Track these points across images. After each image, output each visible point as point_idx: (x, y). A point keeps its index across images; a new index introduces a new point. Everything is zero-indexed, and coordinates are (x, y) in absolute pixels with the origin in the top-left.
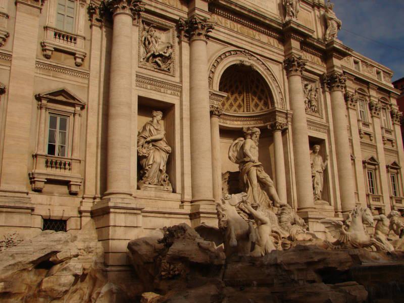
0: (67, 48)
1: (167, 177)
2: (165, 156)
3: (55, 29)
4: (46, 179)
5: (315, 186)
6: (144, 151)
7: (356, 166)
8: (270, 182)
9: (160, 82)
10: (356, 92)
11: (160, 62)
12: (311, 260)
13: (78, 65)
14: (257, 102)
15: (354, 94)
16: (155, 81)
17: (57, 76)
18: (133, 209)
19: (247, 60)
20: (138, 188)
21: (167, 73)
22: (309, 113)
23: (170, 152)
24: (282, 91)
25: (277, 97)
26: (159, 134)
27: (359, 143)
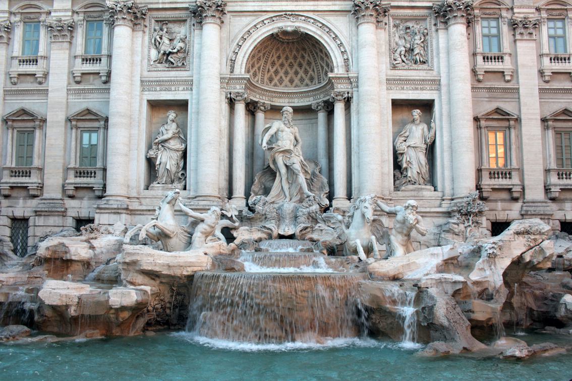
2: (177, 156)
5: (405, 165)
6: (152, 153)
7: (523, 129)
9: (168, 81)
10: (538, 10)
11: (172, 60)
13: (106, 82)
14: (327, 69)
15: (531, 16)
17: (87, 97)
18: (115, 209)
19: (289, 24)
21: (179, 69)
22: (406, 67)
24: (348, 49)
25: (337, 58)
26: (167, 133)
27: (537, 91)
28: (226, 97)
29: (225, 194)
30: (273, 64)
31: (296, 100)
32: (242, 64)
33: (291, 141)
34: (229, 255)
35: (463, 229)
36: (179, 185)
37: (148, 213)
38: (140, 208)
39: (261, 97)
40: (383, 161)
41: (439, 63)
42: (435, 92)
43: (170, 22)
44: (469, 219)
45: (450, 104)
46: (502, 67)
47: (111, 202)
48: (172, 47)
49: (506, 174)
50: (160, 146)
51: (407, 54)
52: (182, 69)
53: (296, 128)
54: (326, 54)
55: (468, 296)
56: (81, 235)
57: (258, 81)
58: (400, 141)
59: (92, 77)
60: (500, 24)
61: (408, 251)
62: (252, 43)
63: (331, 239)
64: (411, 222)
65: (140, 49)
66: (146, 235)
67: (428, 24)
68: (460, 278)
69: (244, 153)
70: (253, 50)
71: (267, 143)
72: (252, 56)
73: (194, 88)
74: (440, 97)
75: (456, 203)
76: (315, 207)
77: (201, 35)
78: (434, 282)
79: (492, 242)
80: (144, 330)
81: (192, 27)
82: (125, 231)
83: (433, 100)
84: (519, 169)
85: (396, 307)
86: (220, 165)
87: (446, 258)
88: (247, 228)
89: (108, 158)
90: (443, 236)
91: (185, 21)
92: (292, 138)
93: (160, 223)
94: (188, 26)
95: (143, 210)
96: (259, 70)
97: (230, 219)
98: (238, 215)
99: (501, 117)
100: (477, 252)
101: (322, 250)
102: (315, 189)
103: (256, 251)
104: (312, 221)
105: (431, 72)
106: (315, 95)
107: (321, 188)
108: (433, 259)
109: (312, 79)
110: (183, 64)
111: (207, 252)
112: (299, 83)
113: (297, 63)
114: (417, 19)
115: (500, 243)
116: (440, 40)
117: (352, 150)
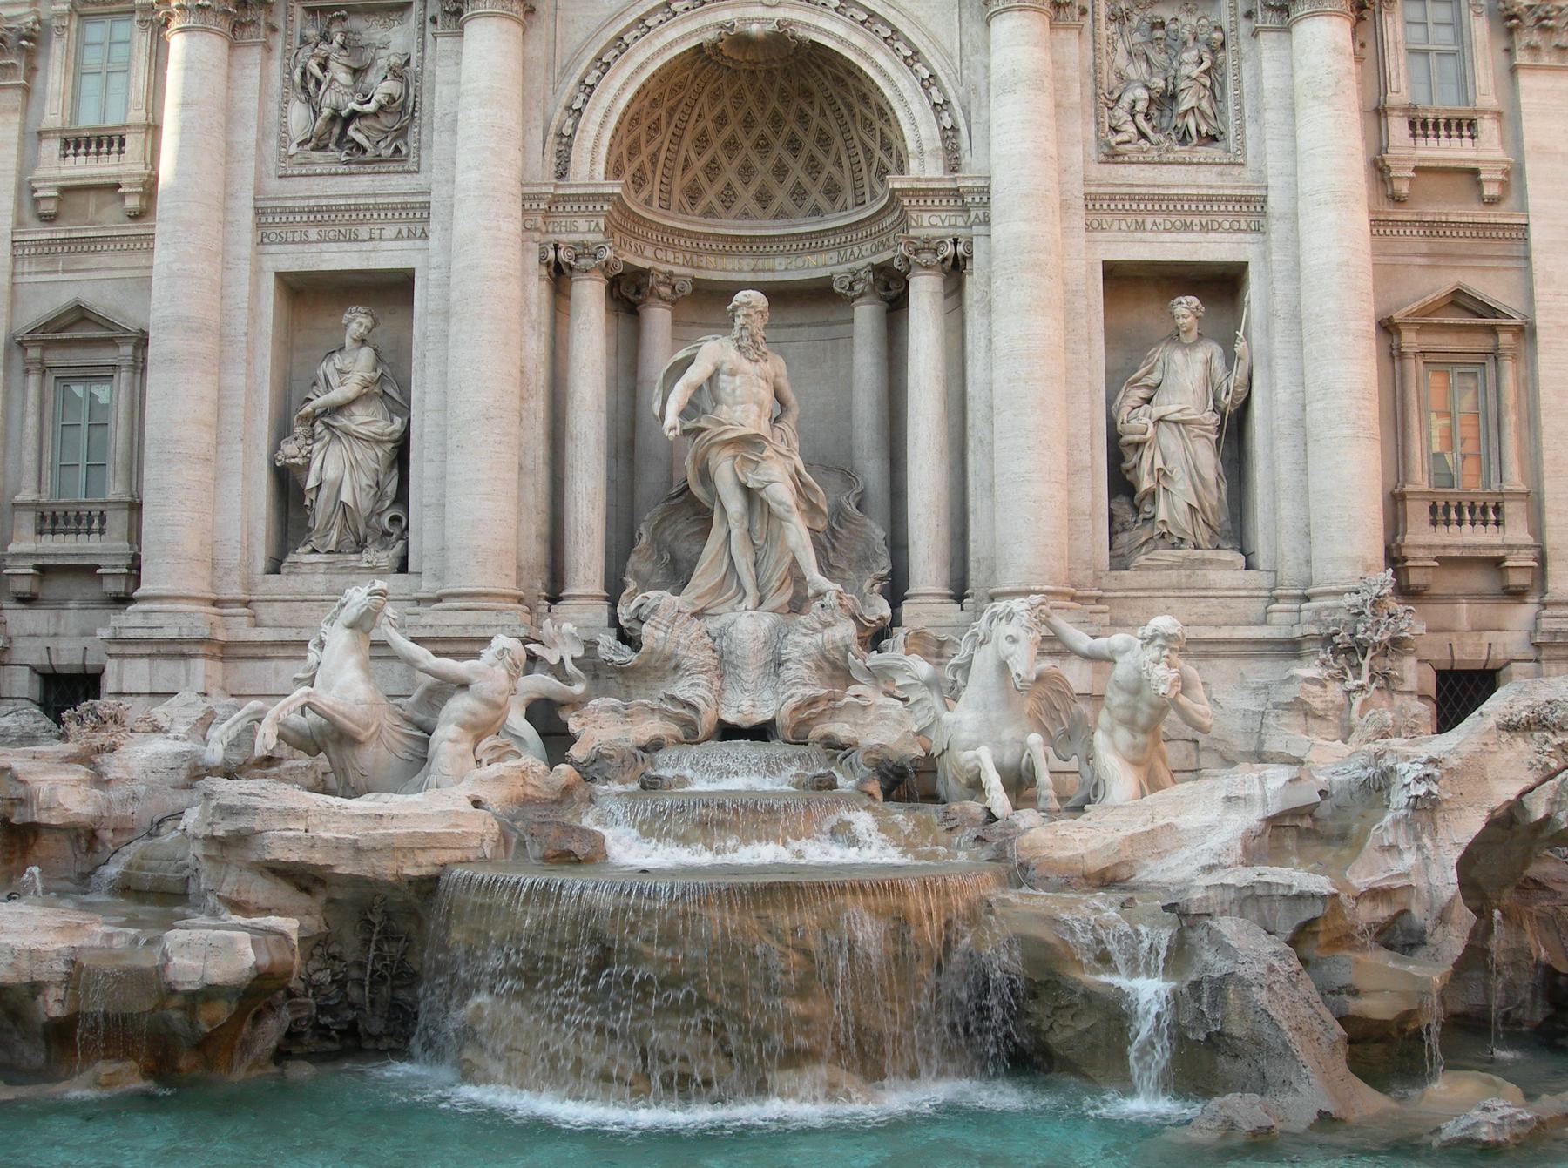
0: (94, 177)
1: (395, 520)
2: (373, 458)
3: (61, 131)
4: (36, 567)
5: (1146, 484)
8: (780, 503)
11: (360, 138)
12: (208, 832)
13: (137, 216)
14: (885, 160)
16: (329, 209)
20: (275, 568)
21: (384, 167)
23: (396, 436)
26: (342, 384)
28: (542, 259)
29: (539, 586)
30: (702, 141)
31: (779, 262)
32: (595, 146)
33: (760, 405)
34: (554, 802)
35: (1340, 699)
36: (383, 554)
37: (282, 652)
39: (660, 254)
40: (1073, 471)
42: (1248, 237)
44: (1359, 665)
45: (1299, 279)
46: (1472, 155)
47: (155, 620)
48: (359, 97)
49: (1484, 510)
50: (319, 427)
51: (1154, 112)
52: (394, 166)
53: (780, 361)
54: (880, 109)
55: (1345, 939)
56: (63, 737)
57: (648, 202)
58: (1131, 402)
59: (92, 200)
60: (1464, 12)
61: (1152, 783)
62: (631, 78)
63: (896, 737)
64: (1162, 689)
65: (255, 104)
66: (280, 736)
68: (1320, 884)
69: (603, 447)
70: (632, 100)
71: (684, 414)
72: (631, 119)
73: (434, 226)
74: (1265, 256)
75: (1317, 612)
76: (845, 631)
77: (459, 53)
78: (1232, 895)
79: (1425, 757)
80: (281, 1055)
81: (430, 28)
82: (207, 721)
83: (1244, 266)
84: (1527, 494)
85: (1104, 978)
86: (521, 487)
87: (1273, 810)
88: (612, 701)
90: (1270, 721)
92: (766, 395)
93: (326, 697)
95: (263, 644)
96: (654, 159)
97: (558, 670)
98: (584, 657)
99: (1469, 320)
100: (1377, 787)
103: (643, 787)
104: (831, 677)
105: (1237, 170)
106: (845, 245)
107: (864, 561)
108: (1233, 816)
109: (832, 191)
110: (397, 150)
111: (482, 793)
112: (789, 205)
113: (784, 135)
115: (1454, 762)
116: (1264, 65)
117: (970, 432)
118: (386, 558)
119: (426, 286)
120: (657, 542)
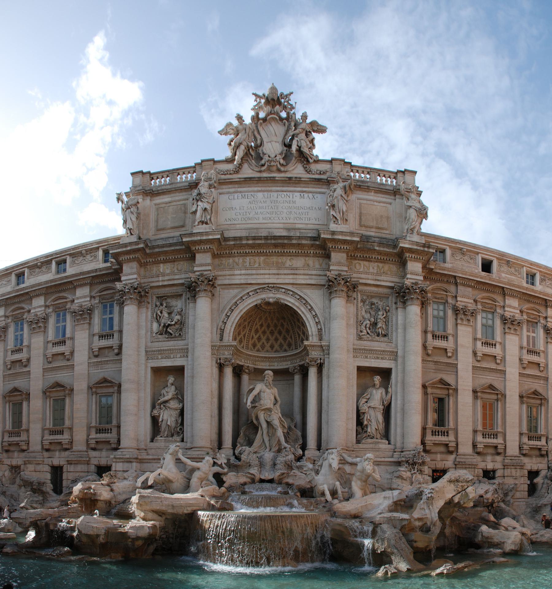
9: (168, 350)
16: (164, 350)
37: (154, 461)
38: (147, 457)
41: (397, 337)
42: (393, 362)
43: (168, 297)
48: (170, 320)
52: (179, 339)
67: (390, 302)
74: (396, 366)
89: (122, 418)
91: (181, 295)
94: (183, 299)
101: (296, 493)
102: (291, 441)
105: (390, 344)
109: (290, 345)
110: (180, 334)
114: (381, 297)
118: (179, 439)
119: (188, 370)
120: (245, 435)
